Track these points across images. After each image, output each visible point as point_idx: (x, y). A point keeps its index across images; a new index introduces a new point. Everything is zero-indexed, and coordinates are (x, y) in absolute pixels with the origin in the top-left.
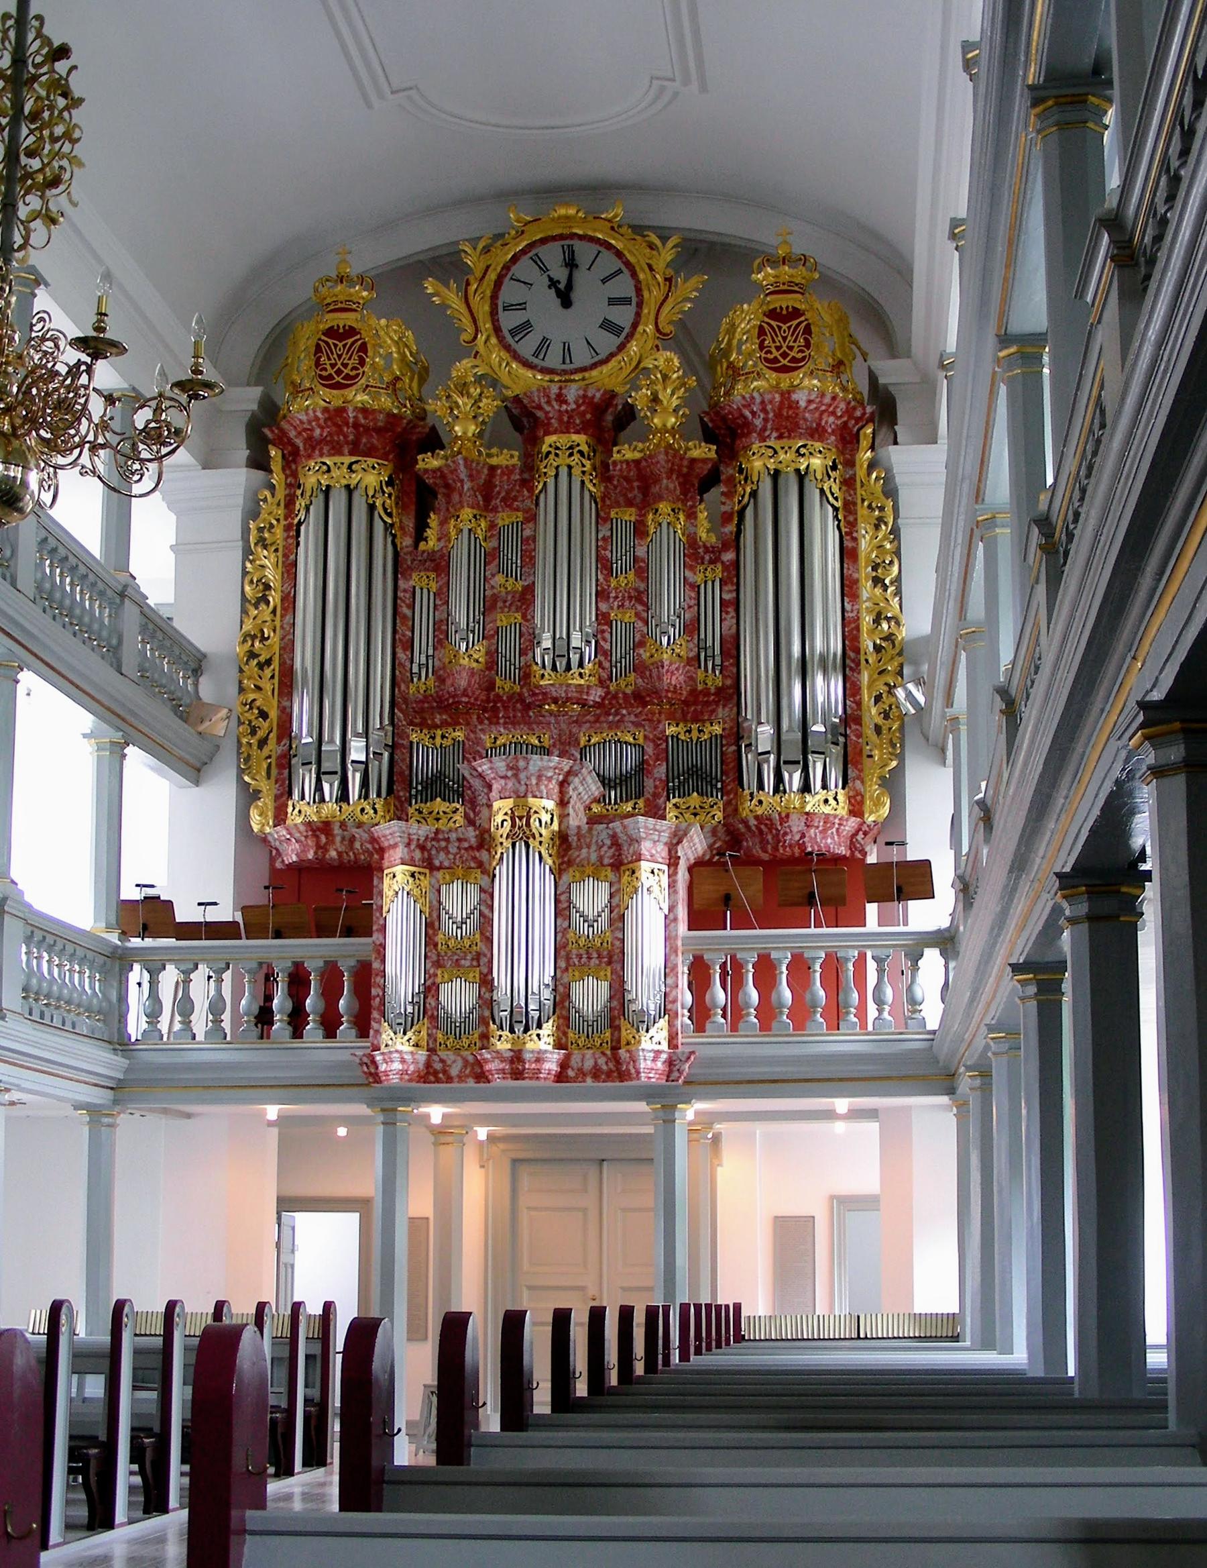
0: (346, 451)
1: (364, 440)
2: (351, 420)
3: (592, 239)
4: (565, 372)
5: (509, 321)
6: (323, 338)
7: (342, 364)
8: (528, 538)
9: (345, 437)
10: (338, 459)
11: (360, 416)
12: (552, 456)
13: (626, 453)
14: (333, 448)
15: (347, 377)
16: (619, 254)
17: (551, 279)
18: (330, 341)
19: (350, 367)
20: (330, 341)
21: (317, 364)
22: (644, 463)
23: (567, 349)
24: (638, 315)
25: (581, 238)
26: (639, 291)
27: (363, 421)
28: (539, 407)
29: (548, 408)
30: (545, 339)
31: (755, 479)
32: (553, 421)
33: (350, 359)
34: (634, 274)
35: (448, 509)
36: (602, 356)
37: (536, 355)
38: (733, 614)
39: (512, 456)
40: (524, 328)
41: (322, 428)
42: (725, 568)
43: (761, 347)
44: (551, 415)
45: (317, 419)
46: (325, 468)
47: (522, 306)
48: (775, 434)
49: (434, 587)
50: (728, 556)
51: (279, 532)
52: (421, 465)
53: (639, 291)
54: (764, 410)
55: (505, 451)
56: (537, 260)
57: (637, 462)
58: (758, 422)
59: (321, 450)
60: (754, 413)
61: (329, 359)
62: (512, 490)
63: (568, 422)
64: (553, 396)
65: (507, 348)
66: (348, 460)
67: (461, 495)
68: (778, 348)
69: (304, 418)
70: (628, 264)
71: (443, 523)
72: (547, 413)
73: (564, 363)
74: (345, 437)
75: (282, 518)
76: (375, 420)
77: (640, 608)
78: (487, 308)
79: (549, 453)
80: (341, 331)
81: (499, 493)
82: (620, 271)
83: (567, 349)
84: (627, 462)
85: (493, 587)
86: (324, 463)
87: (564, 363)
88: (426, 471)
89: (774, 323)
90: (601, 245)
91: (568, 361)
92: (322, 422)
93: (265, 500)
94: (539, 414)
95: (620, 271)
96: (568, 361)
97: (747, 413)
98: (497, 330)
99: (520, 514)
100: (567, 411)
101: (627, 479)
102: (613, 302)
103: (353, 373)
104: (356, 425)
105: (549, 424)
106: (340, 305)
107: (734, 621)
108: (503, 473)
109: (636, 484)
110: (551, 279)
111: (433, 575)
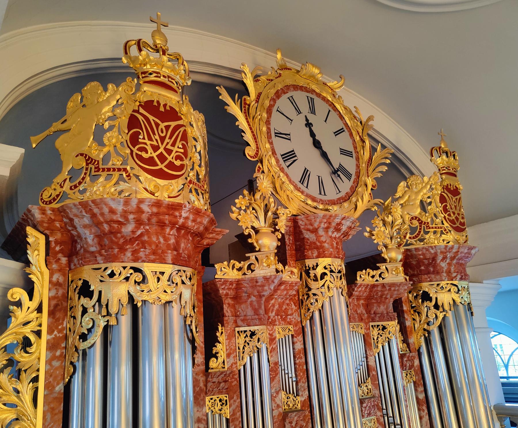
0: (169, 257)
1: (182, 245)
2: (181, 221)
3: (324, 99)
4: (322, 202)
5: (282, 146)
6: (142, 110)
7: (165, 149)
8: (299, 351)
9: (166, 239)
10: (158, 267)
11: (191, 217)
12: (326, 278)
13: (365, 277)
14: (154, 253)
15: (171, 166)
16: (341, 117)
17: (307, 120)
18: (151, 118)
19: (173, 154)
20: (151, 118)
21: (134, 140)
22: (379, 288)
23: (321, 183)
24: (358, 166)
25: (319, 95)
26: (355, 148)
27: (190, 223)
28: (315, 231)
29: (321, 232)
30: (306, 171)
31: (447, 307)
32: (326, 245)
33: (173, 145)
34: (351, 135)
35: (235, 322)
36: (342, 194)
37: (302, 181)
38: (426, 411)
39: (292, 272)
40: (290, 157)
41: (139, 223)
42: (416, 374)
43: (445, 210)
44: (323, 239)
45: (139, 211)
46: (138, 277)
47: (286, 136)
48: (459, 277)
49: (227, 412)
50: (417, 362)
51: (41, 348)
52: (219, 275)
53: (355, 148)
54: (452, 259)
55: (286, 267)
56: (292, 100)
57: (373, 286)
58: (444, 265)
59: (135, 252)
60: (444, 258)
61: (150, 139)
62: (284, 302)
63: (337, 248)
64: (334, 224)
65: (282, 170)
66: (168, 269)
67: (256, 312)
68: (454, 213)
69: (120, 208)
70: (346, 124)
71: (231, 336)
72: (318, 237)
73: (320, 194)
74: (166, 239)
75: (44, 329)
76: (201, 223)
77: (379, 414)
78: (264, 129)
79: (323, 275)
80: (162, 109)
81: (273, 305)
82: (341, 131)
83: (321, 183)
84: (368, 285)
85: (278, 406)
86: (137, 270)
87: (320, 194)
88: (226, 281)
89: (449, 195)
90: (330, 105)
91: (323, 193)
92: (144, 217)
93: (19, 304)
94: (307, 235)
95: (341, 131)
96: (323, 193)
97: (440, 257)
98: (274, 153)
99: (290, 327)
100: (335, 238)
101: (358, 299)
102: (344, 152)
103: (178, 163)
104: (183, 227)
105: (322, 247)
106: (162, 79)
107: (427, 417)
108: (285, 289)
109: (362, 302)
110: (307, 120)
111: (224, 397)
